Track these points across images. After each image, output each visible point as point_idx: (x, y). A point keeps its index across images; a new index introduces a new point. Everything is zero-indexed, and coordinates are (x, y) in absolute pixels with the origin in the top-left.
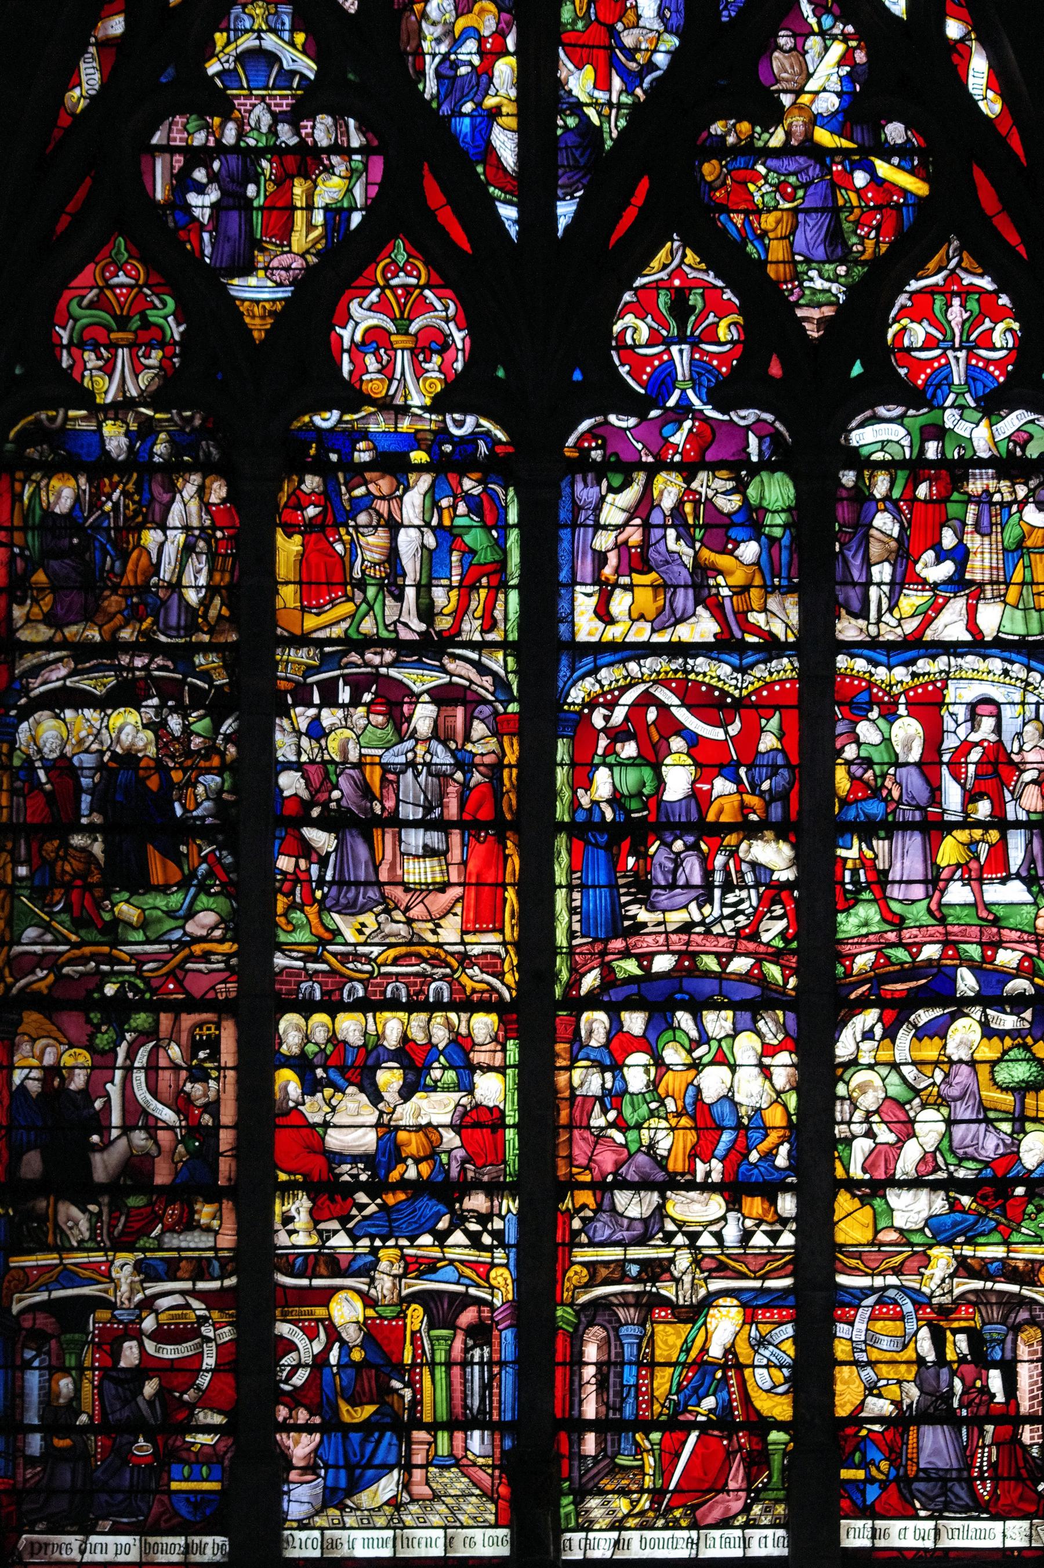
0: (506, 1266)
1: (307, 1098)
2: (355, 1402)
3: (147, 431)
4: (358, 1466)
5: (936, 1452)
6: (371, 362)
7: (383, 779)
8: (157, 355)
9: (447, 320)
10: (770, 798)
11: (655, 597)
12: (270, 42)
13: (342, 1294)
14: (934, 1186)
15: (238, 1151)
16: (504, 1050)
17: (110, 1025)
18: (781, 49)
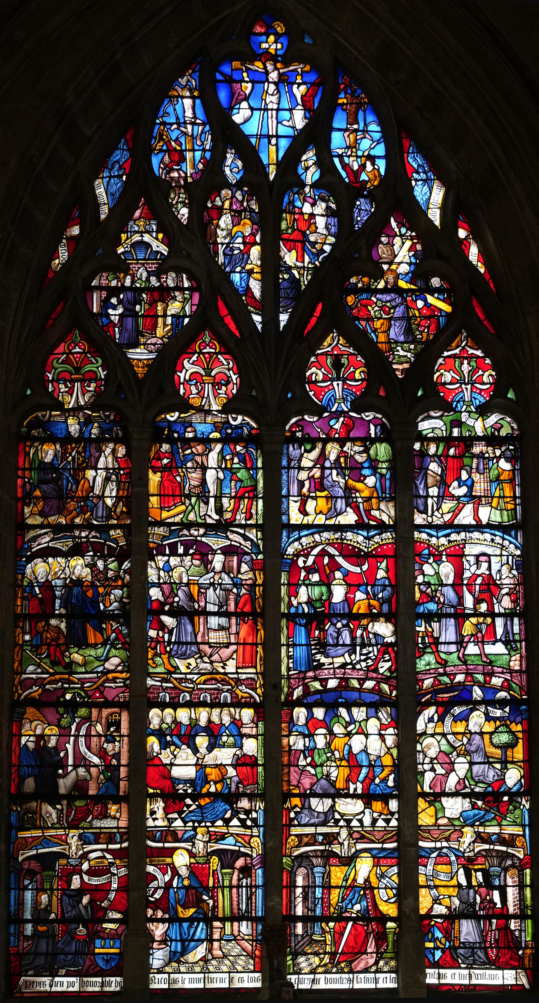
0: (258, 836)
1: (163, 751)
2: (185, 907)
3: (88, 422)
4: (187, 940)
5: (468, 934)
6: (193, 389)
7: (199, 592)
8: (93, 385)
9: (229, 370)
10: (383, 601)
11: (327, 503)
12: (147, 238)
13: (179, 851)
14: (464, 796)
15: (129, 777)
16: (257, 727)
17: (68, 714)
18: (382, 243)
